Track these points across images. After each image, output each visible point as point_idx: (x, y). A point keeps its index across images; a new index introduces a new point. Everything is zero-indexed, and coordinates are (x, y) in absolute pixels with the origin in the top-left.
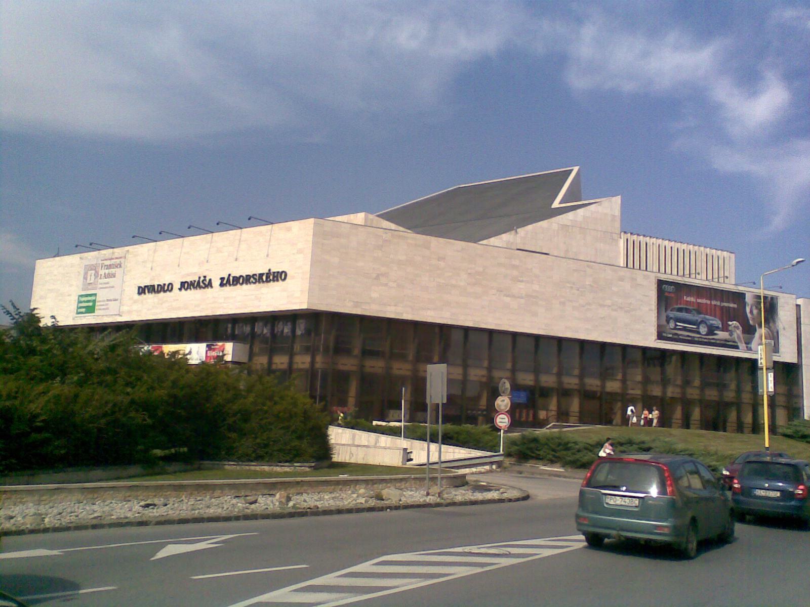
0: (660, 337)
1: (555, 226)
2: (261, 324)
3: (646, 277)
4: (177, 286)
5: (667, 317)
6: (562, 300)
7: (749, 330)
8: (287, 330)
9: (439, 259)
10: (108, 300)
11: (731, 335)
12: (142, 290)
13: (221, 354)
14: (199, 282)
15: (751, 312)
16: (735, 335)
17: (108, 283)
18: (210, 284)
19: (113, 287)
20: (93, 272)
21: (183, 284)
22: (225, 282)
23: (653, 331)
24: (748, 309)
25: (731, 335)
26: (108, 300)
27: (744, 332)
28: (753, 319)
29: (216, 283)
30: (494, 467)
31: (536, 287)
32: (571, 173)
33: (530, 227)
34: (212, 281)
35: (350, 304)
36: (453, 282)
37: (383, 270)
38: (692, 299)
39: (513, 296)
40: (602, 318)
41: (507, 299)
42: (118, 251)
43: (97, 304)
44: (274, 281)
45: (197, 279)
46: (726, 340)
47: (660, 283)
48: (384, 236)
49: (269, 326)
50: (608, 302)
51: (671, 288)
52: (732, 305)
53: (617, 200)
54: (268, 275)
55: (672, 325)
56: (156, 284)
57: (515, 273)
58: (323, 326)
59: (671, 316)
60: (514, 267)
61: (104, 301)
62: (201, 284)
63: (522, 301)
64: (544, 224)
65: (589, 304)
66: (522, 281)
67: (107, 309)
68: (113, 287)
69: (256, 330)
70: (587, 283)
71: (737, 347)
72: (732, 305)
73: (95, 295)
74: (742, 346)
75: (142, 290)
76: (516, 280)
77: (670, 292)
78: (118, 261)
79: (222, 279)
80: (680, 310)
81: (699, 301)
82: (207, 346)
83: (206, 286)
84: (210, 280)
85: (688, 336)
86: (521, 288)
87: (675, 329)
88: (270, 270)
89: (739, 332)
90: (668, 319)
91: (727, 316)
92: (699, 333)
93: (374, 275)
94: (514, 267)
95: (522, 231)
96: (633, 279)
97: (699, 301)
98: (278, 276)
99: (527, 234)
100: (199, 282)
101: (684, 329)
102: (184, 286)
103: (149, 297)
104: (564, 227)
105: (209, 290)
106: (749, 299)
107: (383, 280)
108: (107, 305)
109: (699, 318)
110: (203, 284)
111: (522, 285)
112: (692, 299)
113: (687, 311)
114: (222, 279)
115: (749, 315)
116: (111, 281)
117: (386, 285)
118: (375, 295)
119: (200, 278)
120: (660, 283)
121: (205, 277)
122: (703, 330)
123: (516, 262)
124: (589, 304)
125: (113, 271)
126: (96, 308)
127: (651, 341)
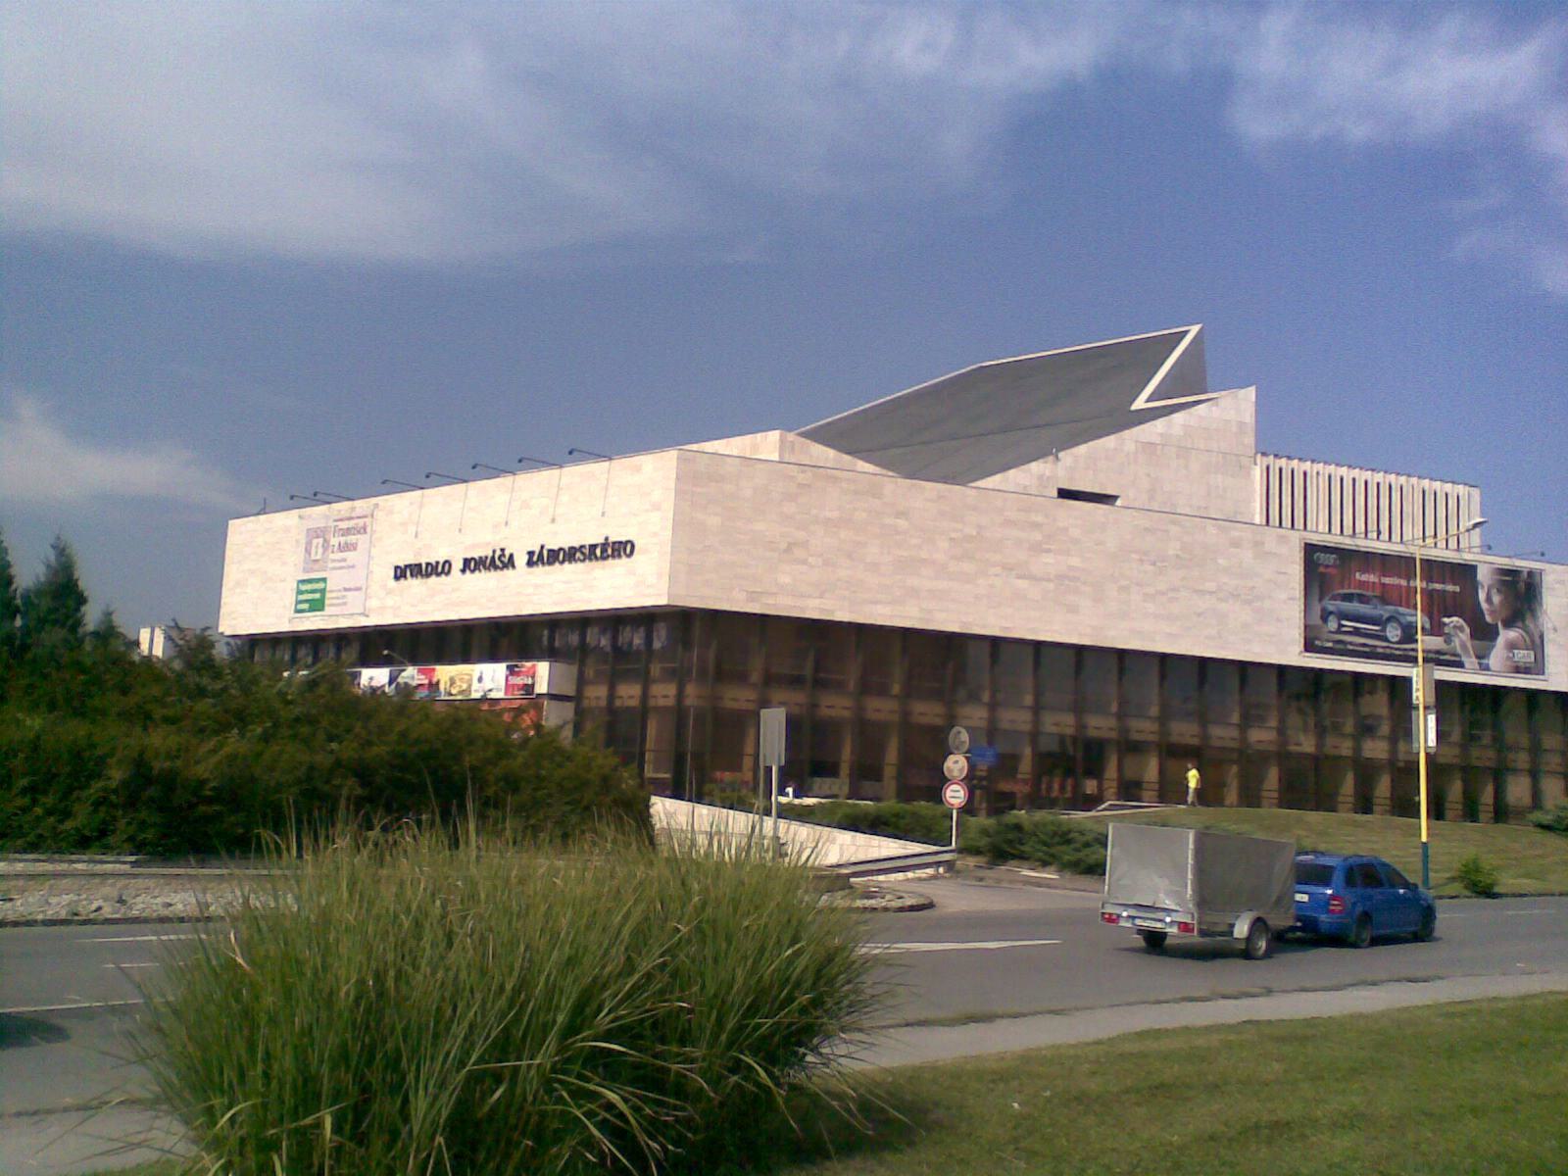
0: (1310, 646)
1: (1130, 446)
2: (596, 630)
3: (1282, 539)
4: (458, 565)
5: (1324, 610)
6: (1124, 583)
7: (1484, 634)
8: (638, 641)
9: (899, 515)
10: (346, 590)
11: (1448, 641)
12: (400, 573)
13: (530, 682)
14: (493, 558)
15: (1489, 600)
16: (1457, 642)
17: (344, 560)
18: (510, 563)
19: (353, 567)
20: (321, 540)
21: (467, 562)
22: (535, 558)
23: (1296, 635)
24: (1482, 596)
25: (1448, 641)
26: (346, 590)
27: (1473, 636)
28: (1492, 613)
29: (521, 560)
30: (941, 870)
31: (1075, 561)
32: (1184, 336)
33: (1082, 449)
34: (515, 558)
35: (742, 596)
36: (924, 555)
37: (801, 535)
38: (1372, 578)
40: (1199, 615)
41: (1022, 584)
42: (361, 505)
43: (328, 595)
44: (613, 556)
45: (490, 554)
46: (1438, 652)
47: (1310, 550)
48: (802, 476)
49: (608, 635)
50: (1210, 586)
51: (1331, 558)
52: (1450, 588)
53: (1250, 393)
54: (604, 546)
55: (1332, 625)
56: (423, 561)
57: (1037, 536)
58: (697, 631)
59: (1331, 608)
60: (1036, 526)
61: (340, 591)
62: (498, 563)
63: (1051, 586)
64: (1109, 442)
65: (1175, 589)
66: (1048, 551)
67: (345, 604)
68: (353, 567)
69: (588, 639)
70: (1171, 552)
71: (1460, 665)
72: (1450, 588)
73: (324, 580)
74: (1470, 661)
75: (400, 573)
76: (1037, 549)
77: (1327, 566)
78: (361, 522)
79: (531, 554)
80: (1348, 598)
81: (1387, 580)
82: (508, 667)
83: (505, 566)
84: (511, 556)
85: (1364, 645)
86: (1047, 563)
87: (1339, 631)
88: (607, 539)
89: (1465, 636)
90: (1325, 616)
91: (1438, 608)
92: (1386, 639)
93: (784, 546)
96: (1258, 544)
97: (1387, 580)
98: (619, 549)
99: (1078, 464)
100: (493, 558)
101: (1357, 632)
102: (471, 565)
103: (413, 584)
104: (1149, 447)
105: (509, 573)
106: (1484, 575)
107: (799, 553)
108: (344, 597)
109: (1385, 611)
110: (500, 562)
111: (1049, 559)
112: (1372, 578)
113: (1363, 599)
114: (531, 554)
115: (1484, 606)
116: (349, 555)
117: (804, 562)
118: (785, 579)
119: (494, 552)
120: (1310, 550)
121: (503, 550)
122: (1393, 633)
123: (1039, 519)
124: (1175, 589)
125: (351, 539)
126: (327, 602)
127: (1293, 655)
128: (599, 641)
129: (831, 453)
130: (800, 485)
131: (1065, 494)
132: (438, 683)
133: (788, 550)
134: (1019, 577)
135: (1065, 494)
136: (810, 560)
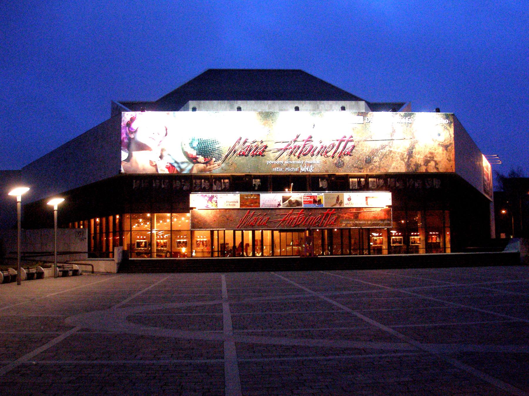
128: (395, 184)
132: (320, 201)
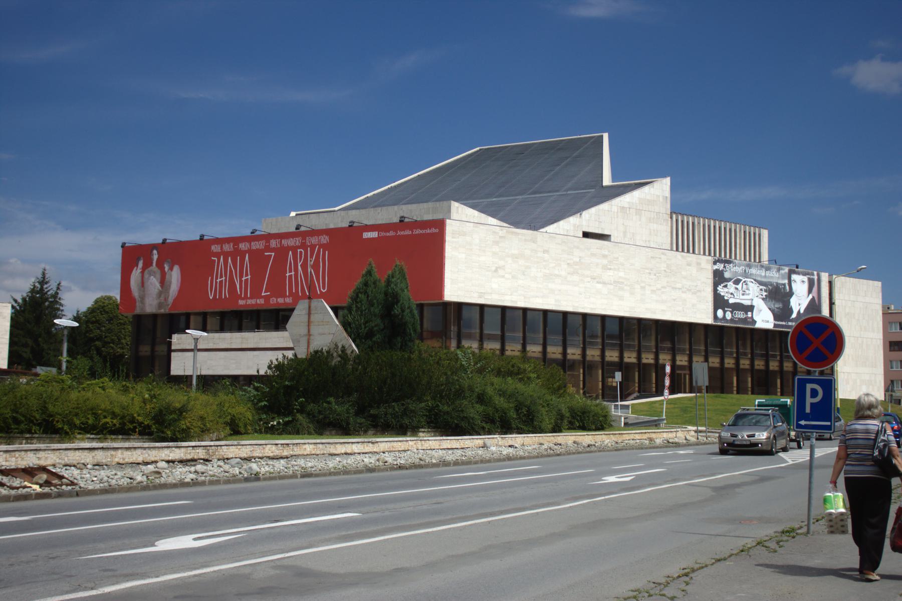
1: (615, 209)
6: (643, 285)
31: (622, 274)
33: (593, 210)
35: (476, 295)
36: (557, 272)
37: (501, 263)
39: (604, 283)
40: (674, 300)
41: (599, 286)
50: (679, 285)
53: (666, 182)
57: (605, 262)
60: (605, 256)
63: (612, 287)
66: (610, 269)
76: (605, 268)
86: (609, 276)
93: (494, 268)
94: (605, 256)
95: (586, 214)
96: (698, 264)
99: (593, 218)
107: (501, 272)
111: (611, 273)
117: (503, 277)
123: (606, 253)
127: (708, 320)
129: (475, 213)
130: (501, 237)
131: (586, 235)
133: (496, 271)
134: (598, 282)
135: (586, 235)
136: (507, 276)
